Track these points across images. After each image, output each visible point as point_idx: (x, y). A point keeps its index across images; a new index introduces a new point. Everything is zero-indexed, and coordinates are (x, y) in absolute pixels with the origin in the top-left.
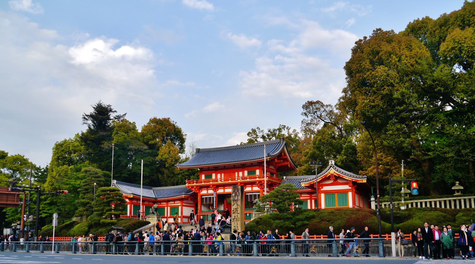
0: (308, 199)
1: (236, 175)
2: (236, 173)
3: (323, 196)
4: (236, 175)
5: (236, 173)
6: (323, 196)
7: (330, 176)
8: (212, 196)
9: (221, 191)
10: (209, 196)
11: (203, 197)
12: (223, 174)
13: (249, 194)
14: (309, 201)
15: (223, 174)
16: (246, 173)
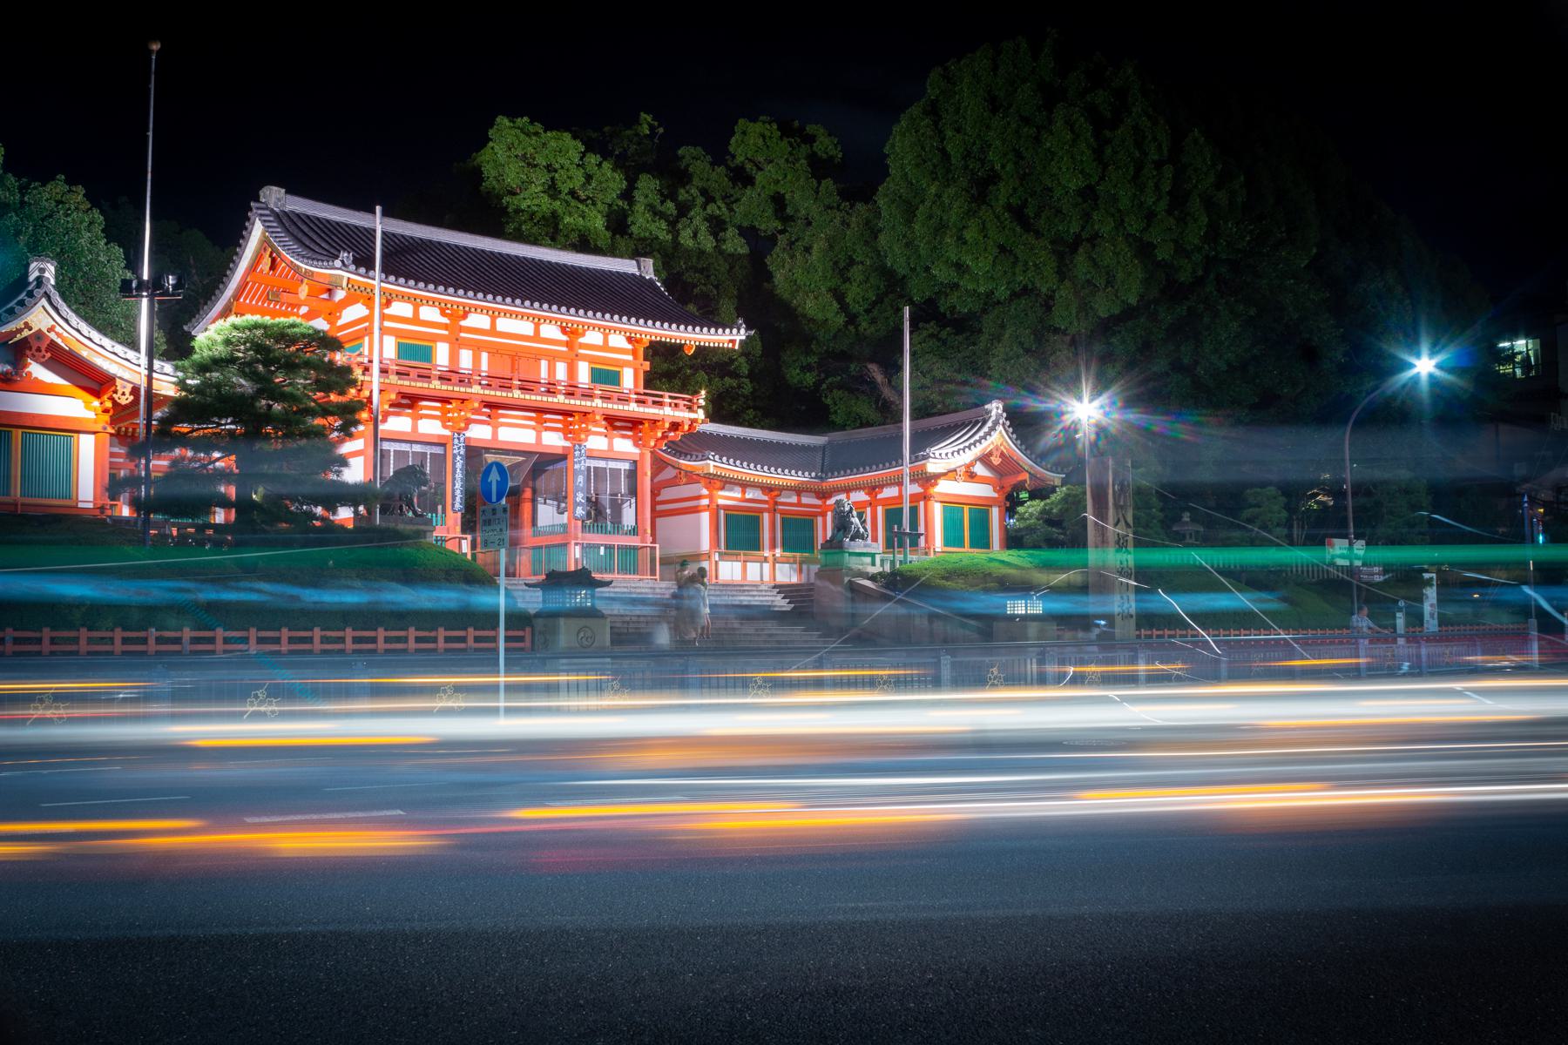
0: (761, 511)
1: (544, 374)
2: (544, 364)
3: (937, 509)
4: (544, 374)
5: (544, 364)
6: (937, 509)
7: (991, 454)
8: (429, 450)
9: (480, 433)
10: (417, 448)
11: (386, 446)
12: (485, 356)
13: (593, 463)
14: (766, 516)
15: (485, 356)
16: (583, 375)
